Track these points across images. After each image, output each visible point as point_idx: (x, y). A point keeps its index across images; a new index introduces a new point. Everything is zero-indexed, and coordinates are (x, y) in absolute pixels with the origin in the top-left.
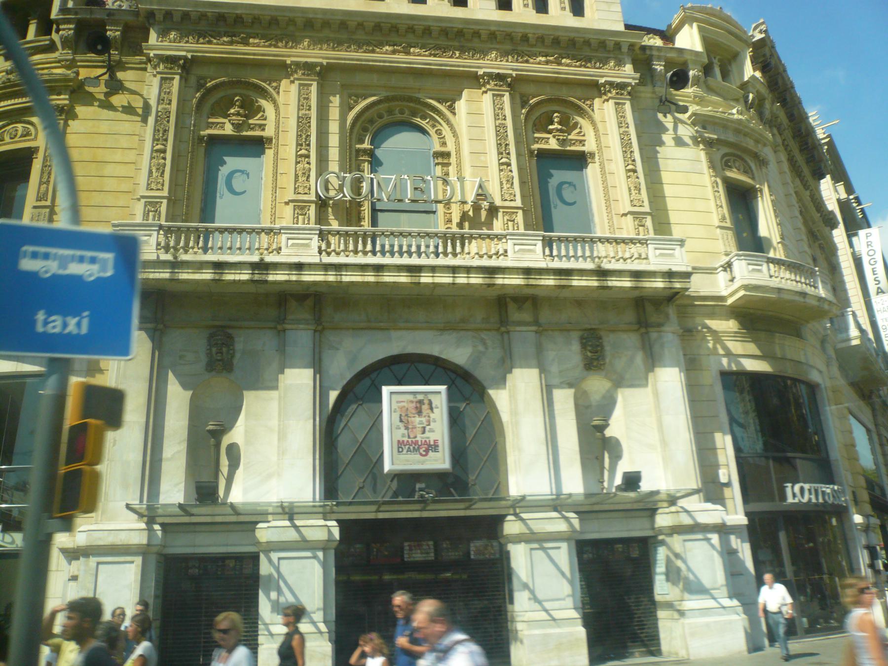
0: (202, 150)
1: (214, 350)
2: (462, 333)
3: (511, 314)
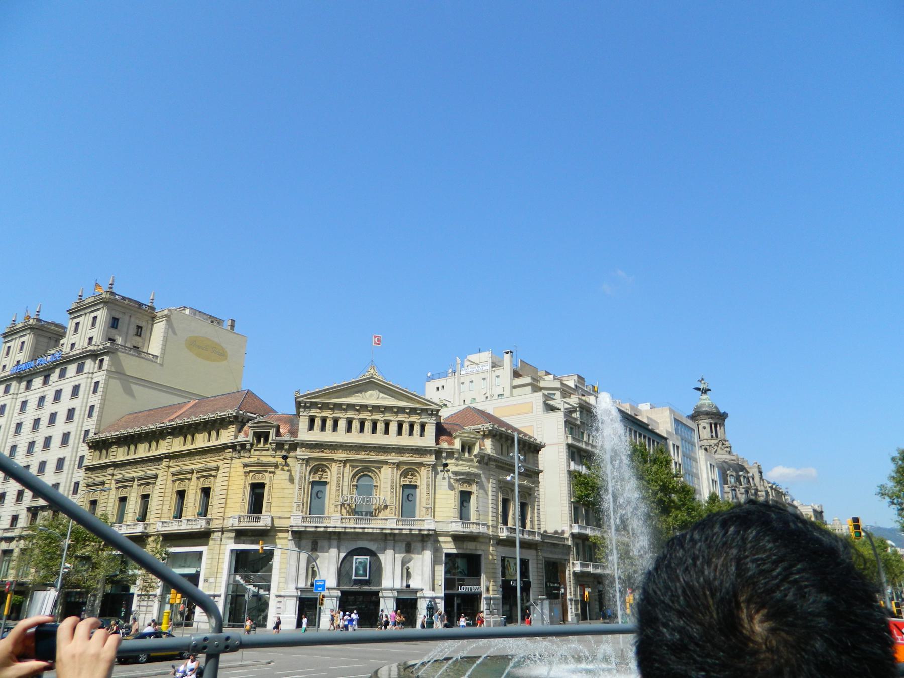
3: (388, 539)
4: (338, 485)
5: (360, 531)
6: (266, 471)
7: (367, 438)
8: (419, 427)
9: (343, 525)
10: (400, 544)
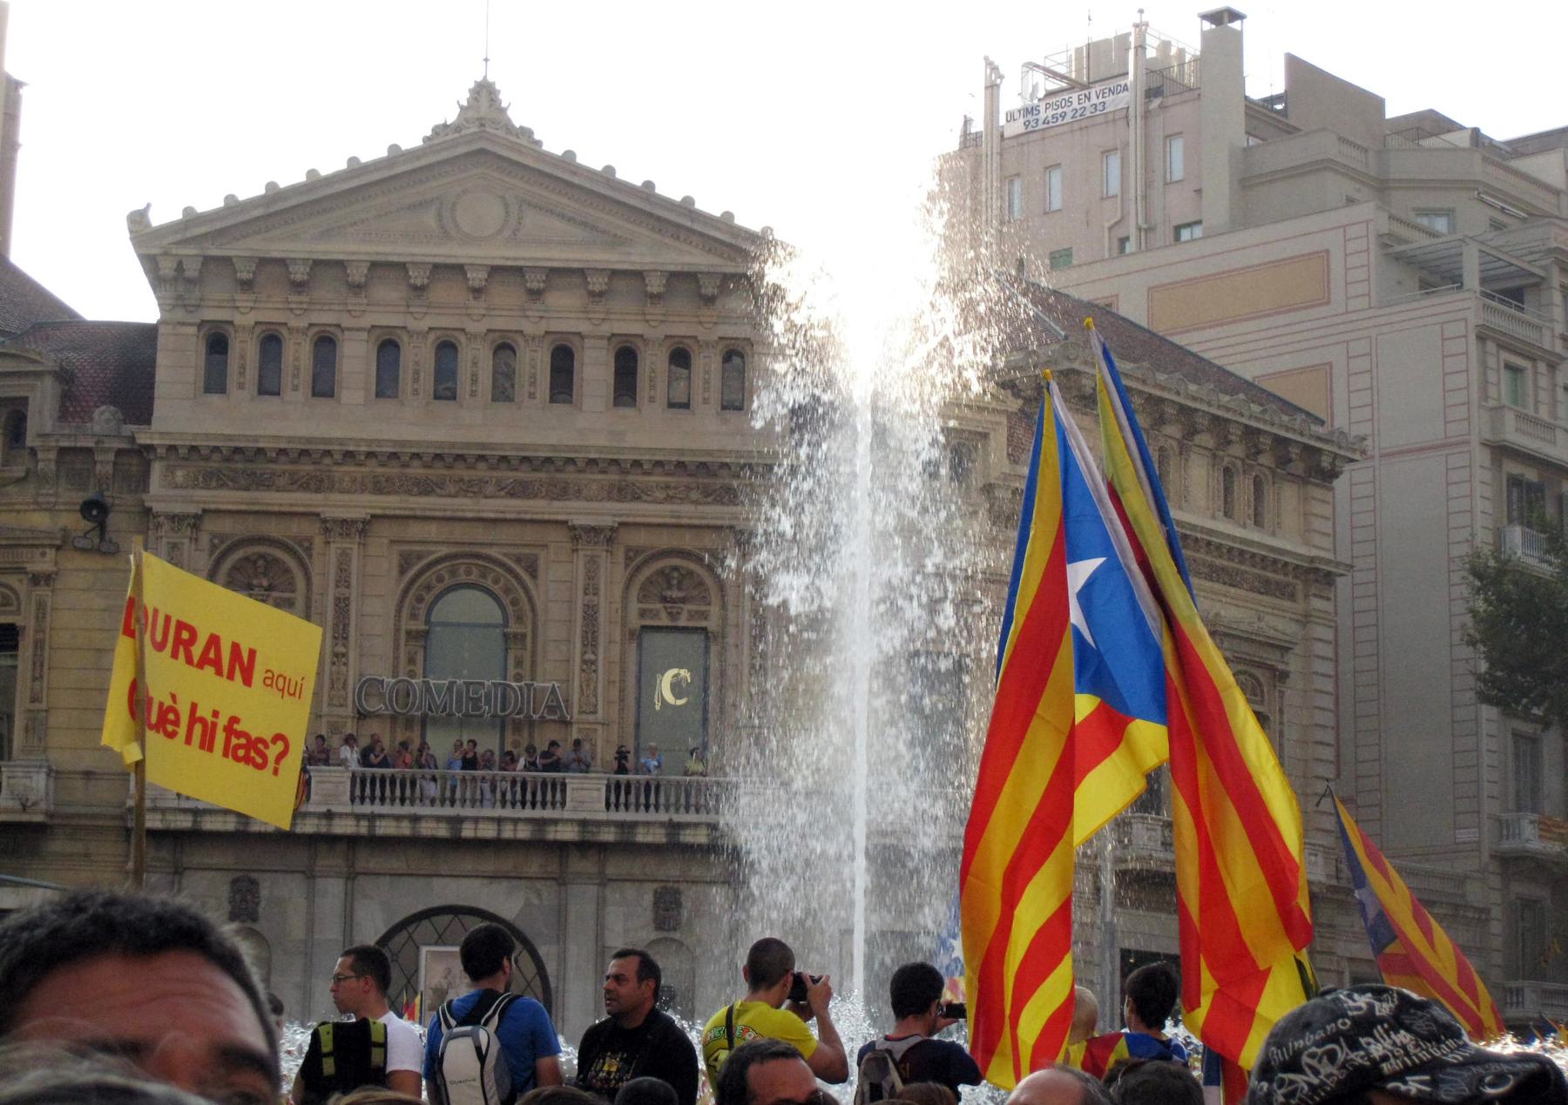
1: (238, 897)
2: (515, 882)
5: (442, 831)
6: (20, 570)
7: (475, 423)
8: (716, 363)
9: (367, 808)
10: (630, 890)
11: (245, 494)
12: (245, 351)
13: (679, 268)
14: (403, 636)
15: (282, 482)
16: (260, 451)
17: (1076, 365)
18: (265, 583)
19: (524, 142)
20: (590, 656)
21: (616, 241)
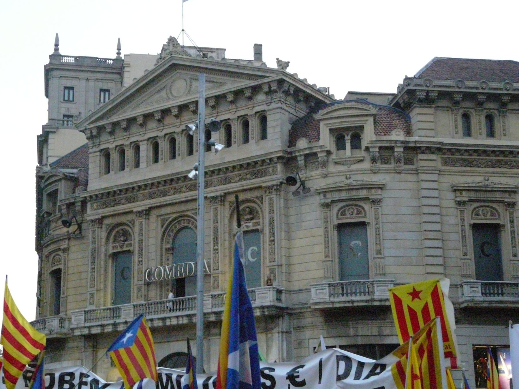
0: (110, 261)
4: (141, 255)
5: (160, 324)
6: (59, 249)
11: (113, 208)
12: (115, 157)
13: (235, 89)
14: (164, 250)
15: (123, 201)
16: (115, 192)
17: (411, 87)
18: (122, 239)
19: (184, 57)
20: (216, 247)
21: (222, 84)
